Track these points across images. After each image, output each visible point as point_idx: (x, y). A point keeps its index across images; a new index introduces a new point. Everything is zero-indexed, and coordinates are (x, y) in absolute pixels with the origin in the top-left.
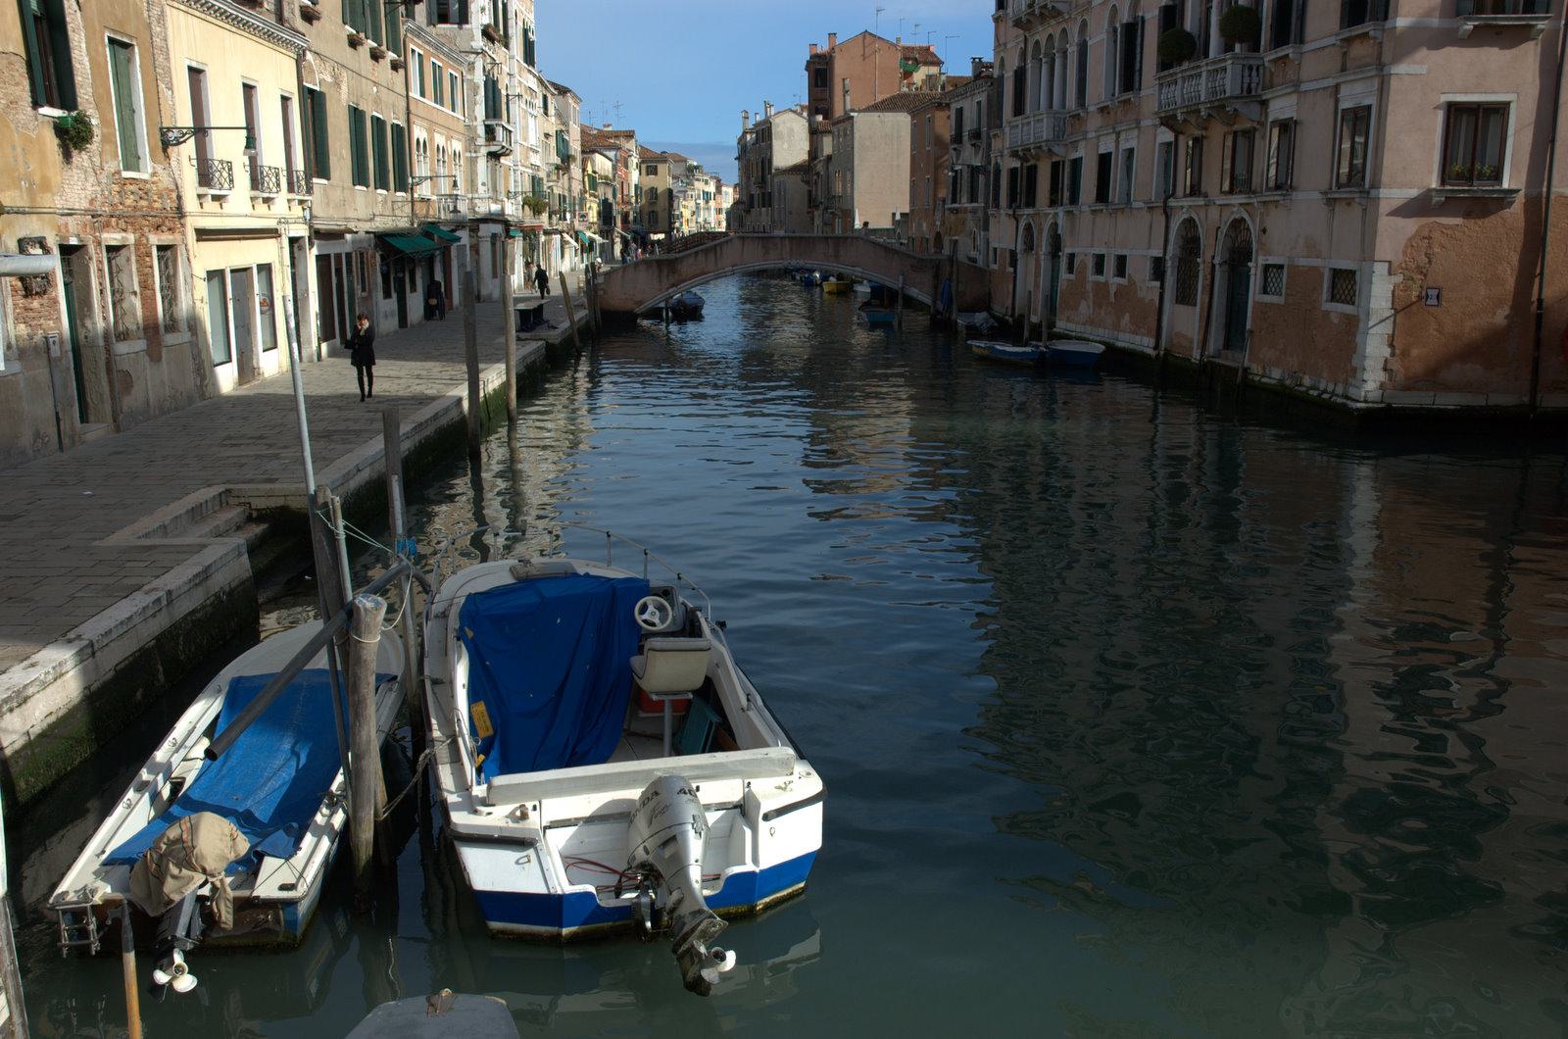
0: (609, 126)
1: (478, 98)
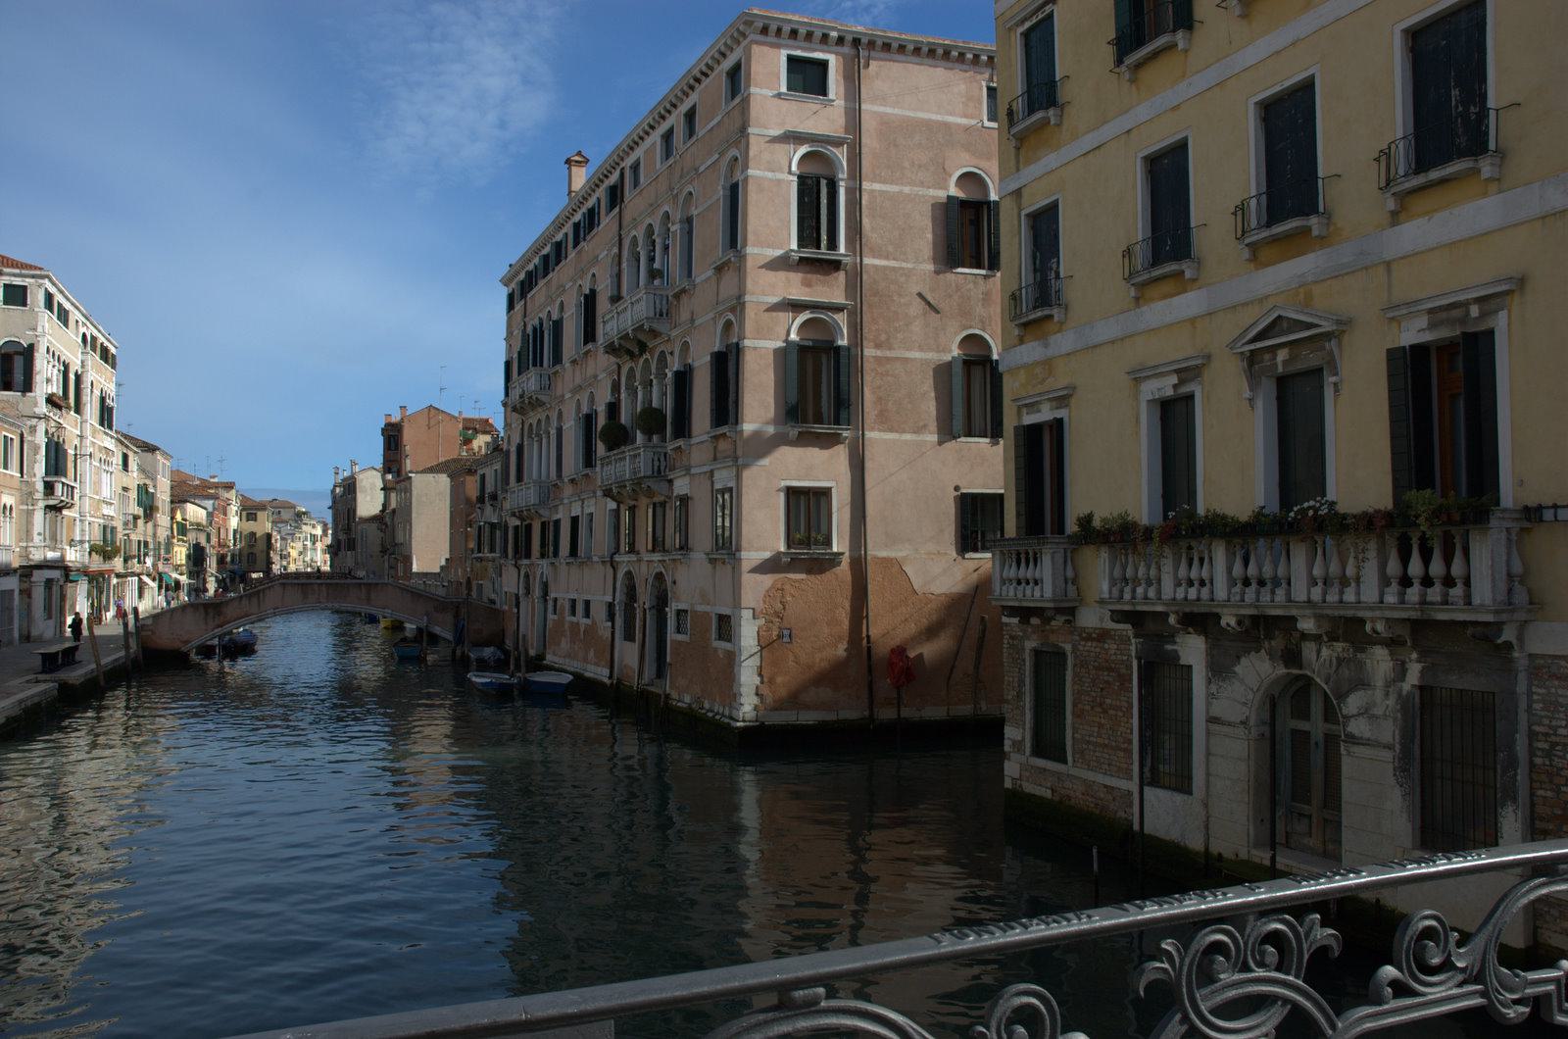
0: (214, 477)
1: (38, 457)
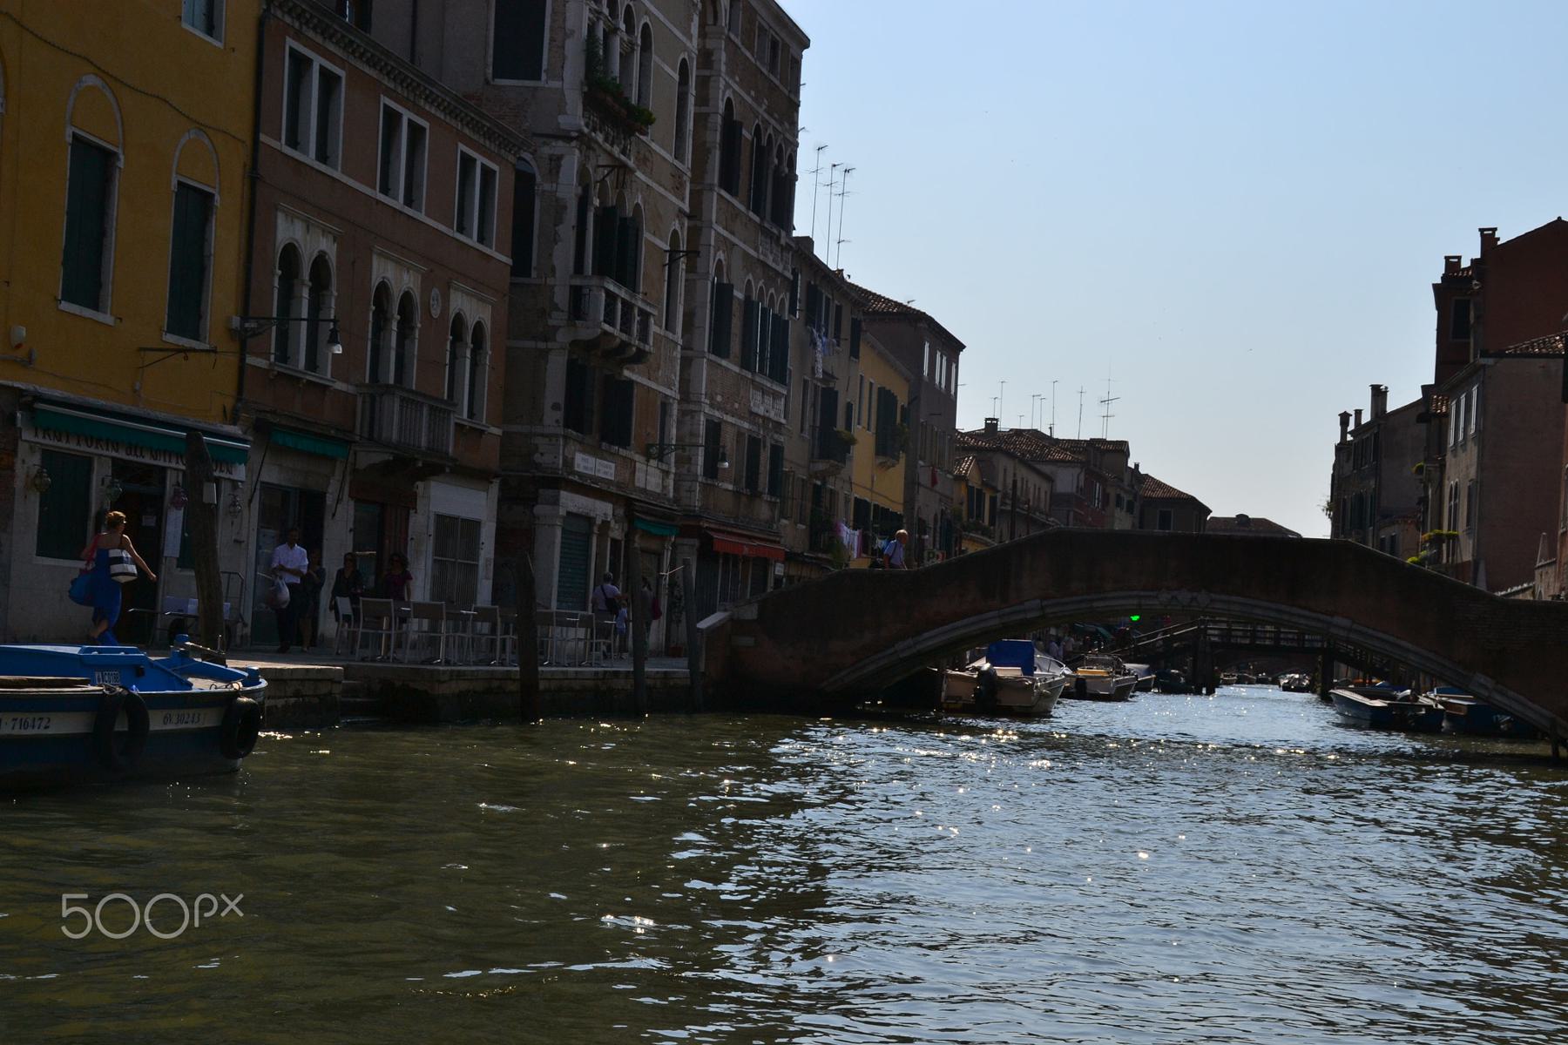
1: (560, 228)
